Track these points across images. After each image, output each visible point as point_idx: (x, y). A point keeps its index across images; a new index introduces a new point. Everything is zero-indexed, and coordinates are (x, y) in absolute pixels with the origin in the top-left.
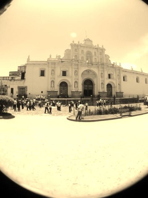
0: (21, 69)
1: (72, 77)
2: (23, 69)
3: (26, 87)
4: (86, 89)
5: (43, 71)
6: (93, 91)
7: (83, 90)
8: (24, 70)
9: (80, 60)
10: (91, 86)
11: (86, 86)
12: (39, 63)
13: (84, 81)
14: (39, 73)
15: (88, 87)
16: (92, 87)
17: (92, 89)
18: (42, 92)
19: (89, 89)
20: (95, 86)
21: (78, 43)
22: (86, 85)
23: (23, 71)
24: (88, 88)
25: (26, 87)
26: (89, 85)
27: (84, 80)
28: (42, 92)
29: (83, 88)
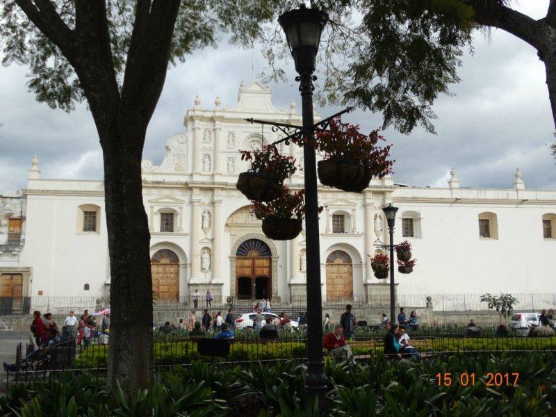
0: (8, 206)
1: (191, 235)
2: (15, 204)
3: (28, 271)
4: (247, 272)
5: (90, 213)
6: (273, 278)
7: (234, 278)
8: (19, 210)
9: (221, 174)
10: (265, 262)
11: (248, 263)
12: (77, 189)
13: (237, 247)
14: (78, 219)
15: (253, 267)
16: (270, 267)
17: (270, 273)
18: (87, 287)
19: (259, 272)
20: (280, 262)
21: (212, 106)
22: (248, 259)
23: (17, 215)
24: (253, 271)
25: (28, 271)
26: (258, 259)
27: (239, 240)
28: (87, 287)
29: (234, 269)
